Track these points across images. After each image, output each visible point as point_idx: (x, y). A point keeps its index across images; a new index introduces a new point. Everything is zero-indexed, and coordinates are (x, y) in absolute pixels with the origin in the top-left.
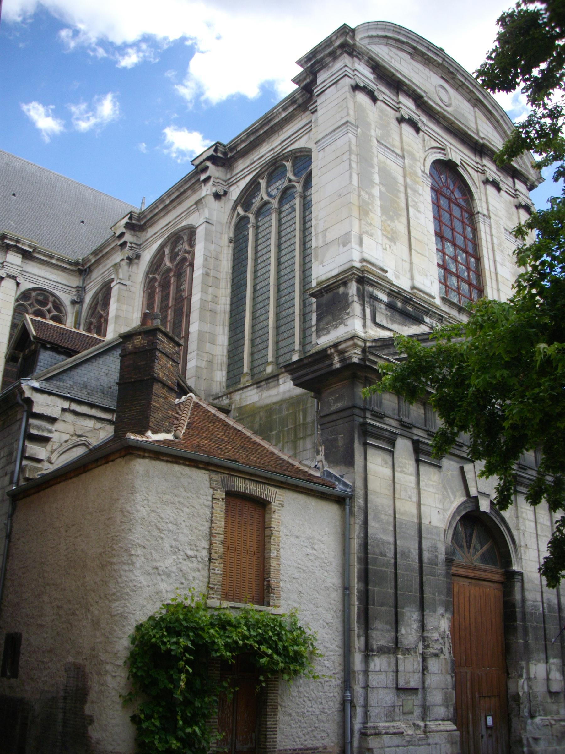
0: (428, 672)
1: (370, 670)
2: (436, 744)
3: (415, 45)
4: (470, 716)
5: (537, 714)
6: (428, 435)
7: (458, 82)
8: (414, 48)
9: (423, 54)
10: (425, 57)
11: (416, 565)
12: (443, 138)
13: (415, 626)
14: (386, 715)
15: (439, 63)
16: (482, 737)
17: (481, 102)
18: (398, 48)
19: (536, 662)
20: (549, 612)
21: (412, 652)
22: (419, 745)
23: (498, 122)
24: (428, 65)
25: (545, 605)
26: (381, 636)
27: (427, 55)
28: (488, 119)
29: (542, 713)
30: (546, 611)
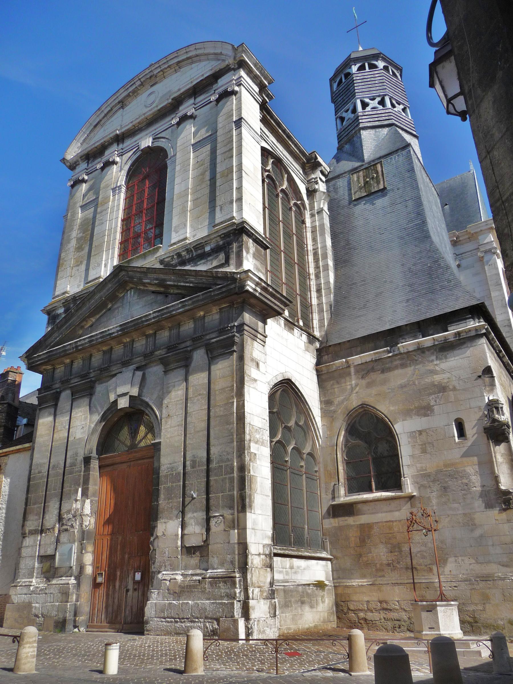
0: (59, 542)
1: (23, 546)
2: (51, 593)
3: (117, 101)
4: (118, 573)
5: (163, 568)
6: (81, 377)
7: (160, 74)
8: (119, 102)
9: (128, 95)
10: (131, 94)
11: (61, 471)
12: (160, 126)
13: (56, 512)
14: (28, 574)
15: (140, 85)
16: (127, 591)
17: (179, 62)
18: (111, 117)
19: (166, 521)
20: (193, 467)
21: (51, 530)
22: (39, 594)
23: (197, 56)
24: (138, 94)
25: (188, 463)
26: (32, 524)
27: (129, 94)
28: (192, 63)
29: (169, 567)
30: (188, 468)
